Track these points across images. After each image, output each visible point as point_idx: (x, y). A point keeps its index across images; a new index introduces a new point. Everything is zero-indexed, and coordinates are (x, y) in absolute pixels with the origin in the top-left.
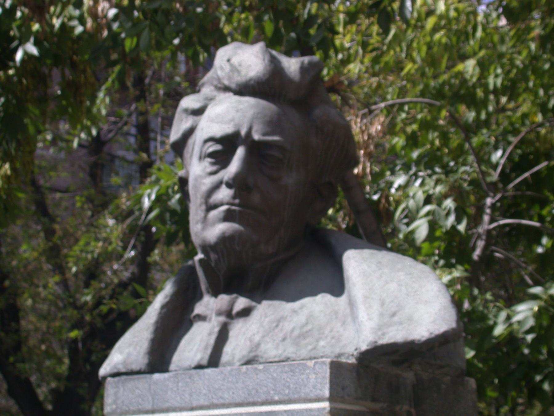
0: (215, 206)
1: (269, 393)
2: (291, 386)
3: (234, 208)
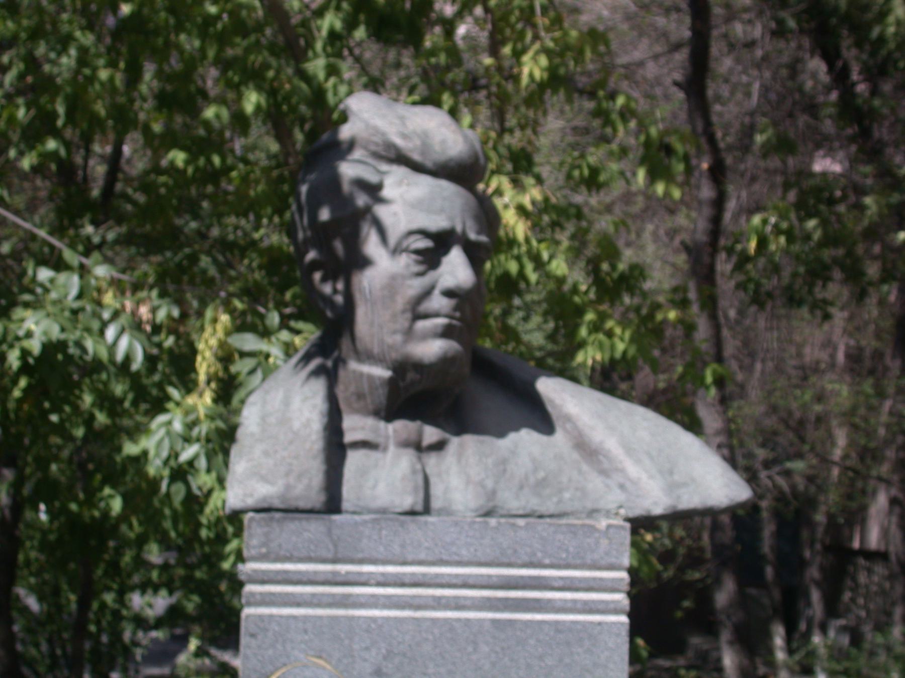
0: (426, 316)
1: (535, 555)
2: (571, 549)
3: (455, 322)
